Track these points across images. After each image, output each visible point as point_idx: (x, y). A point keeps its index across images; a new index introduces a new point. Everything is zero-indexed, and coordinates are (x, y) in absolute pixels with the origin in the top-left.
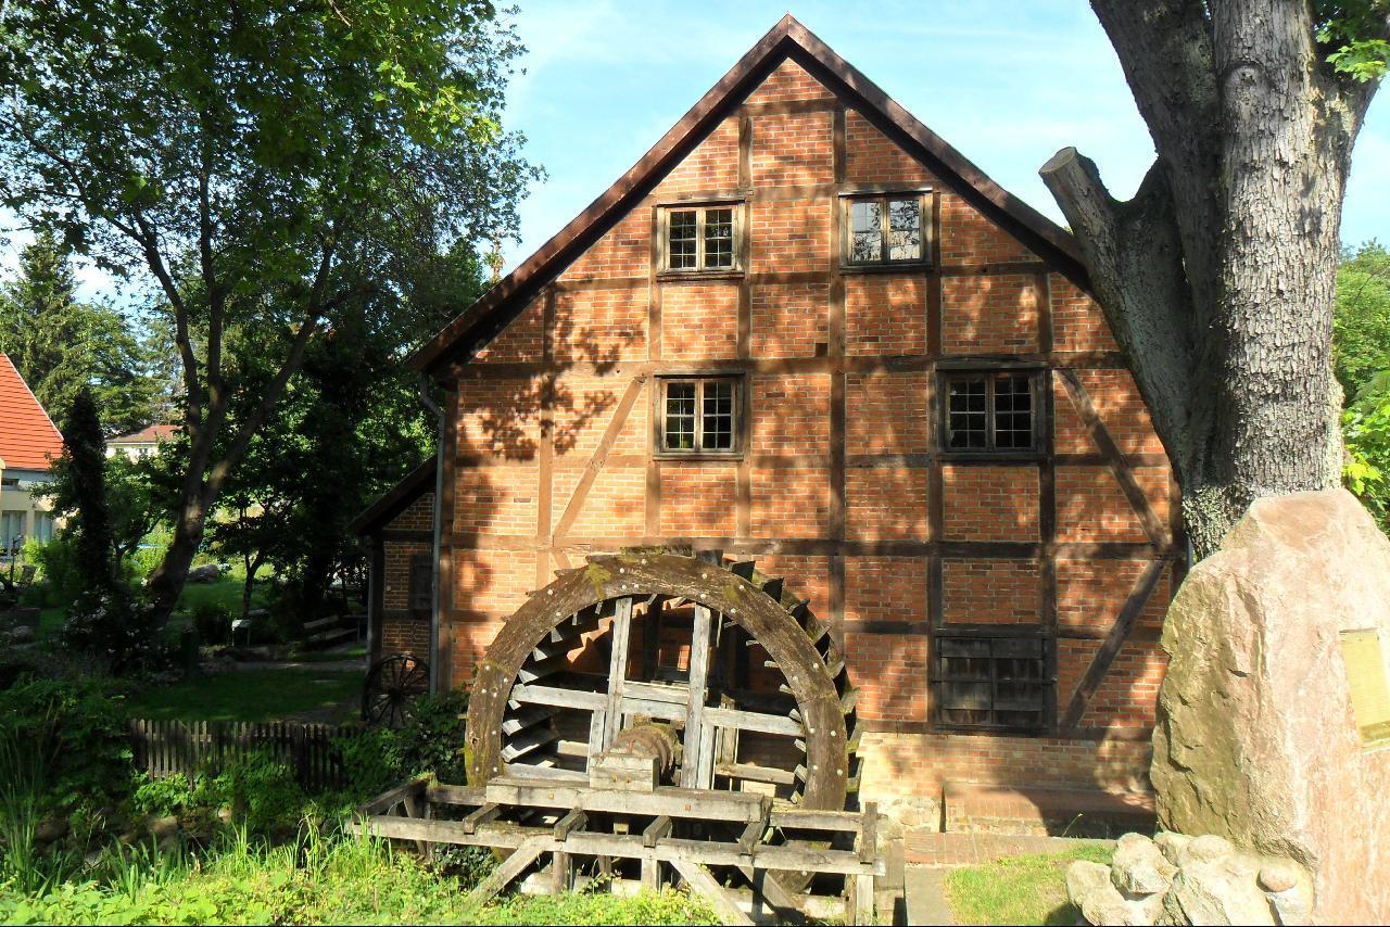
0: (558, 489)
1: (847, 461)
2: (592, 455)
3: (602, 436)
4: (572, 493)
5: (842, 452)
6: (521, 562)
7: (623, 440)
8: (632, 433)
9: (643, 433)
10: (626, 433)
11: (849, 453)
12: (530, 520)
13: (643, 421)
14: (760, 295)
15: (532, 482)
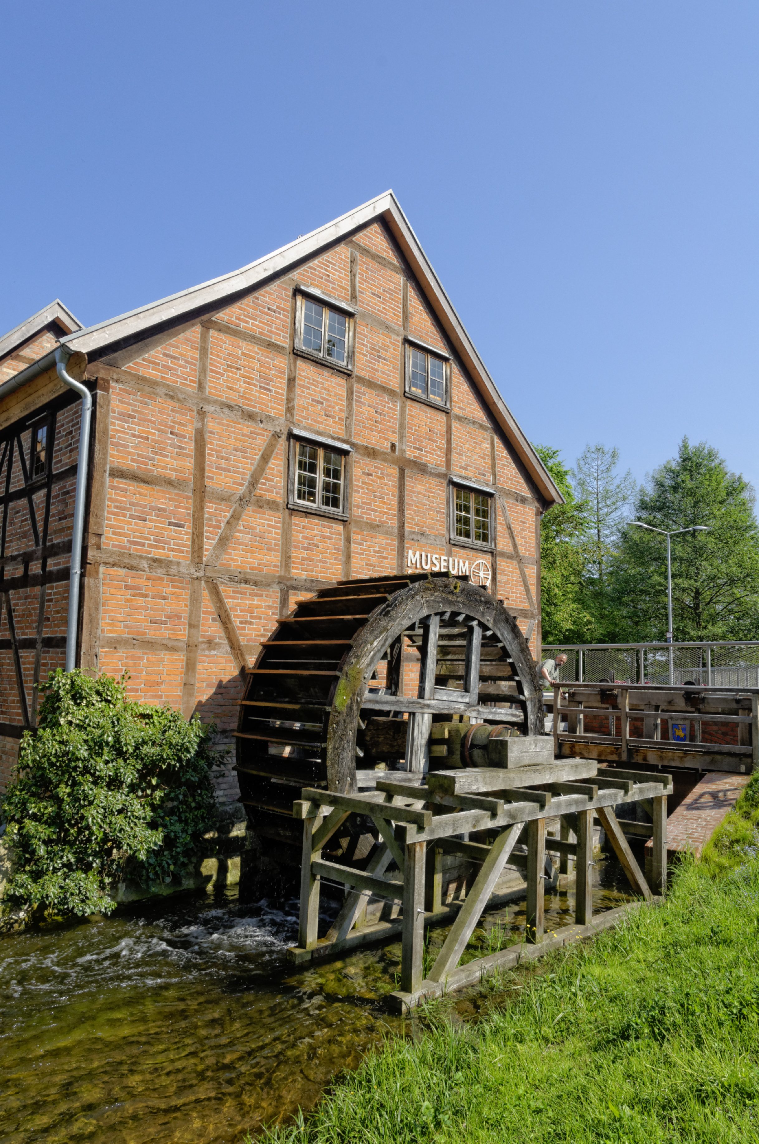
0: (210, 519)
1: (406, 534)
2: (241, 492)
3: (248, 477)
4: (223, 525)
5: (403, 527)
6: (173, 587)
7: (264, 484)
8: (272, 480)
9: (280, 482)
10: (267, 479)
11: (406, 529)
12: (184, 546)
13: (279, 471)
14: (359, 393)
15: (187, 508)
